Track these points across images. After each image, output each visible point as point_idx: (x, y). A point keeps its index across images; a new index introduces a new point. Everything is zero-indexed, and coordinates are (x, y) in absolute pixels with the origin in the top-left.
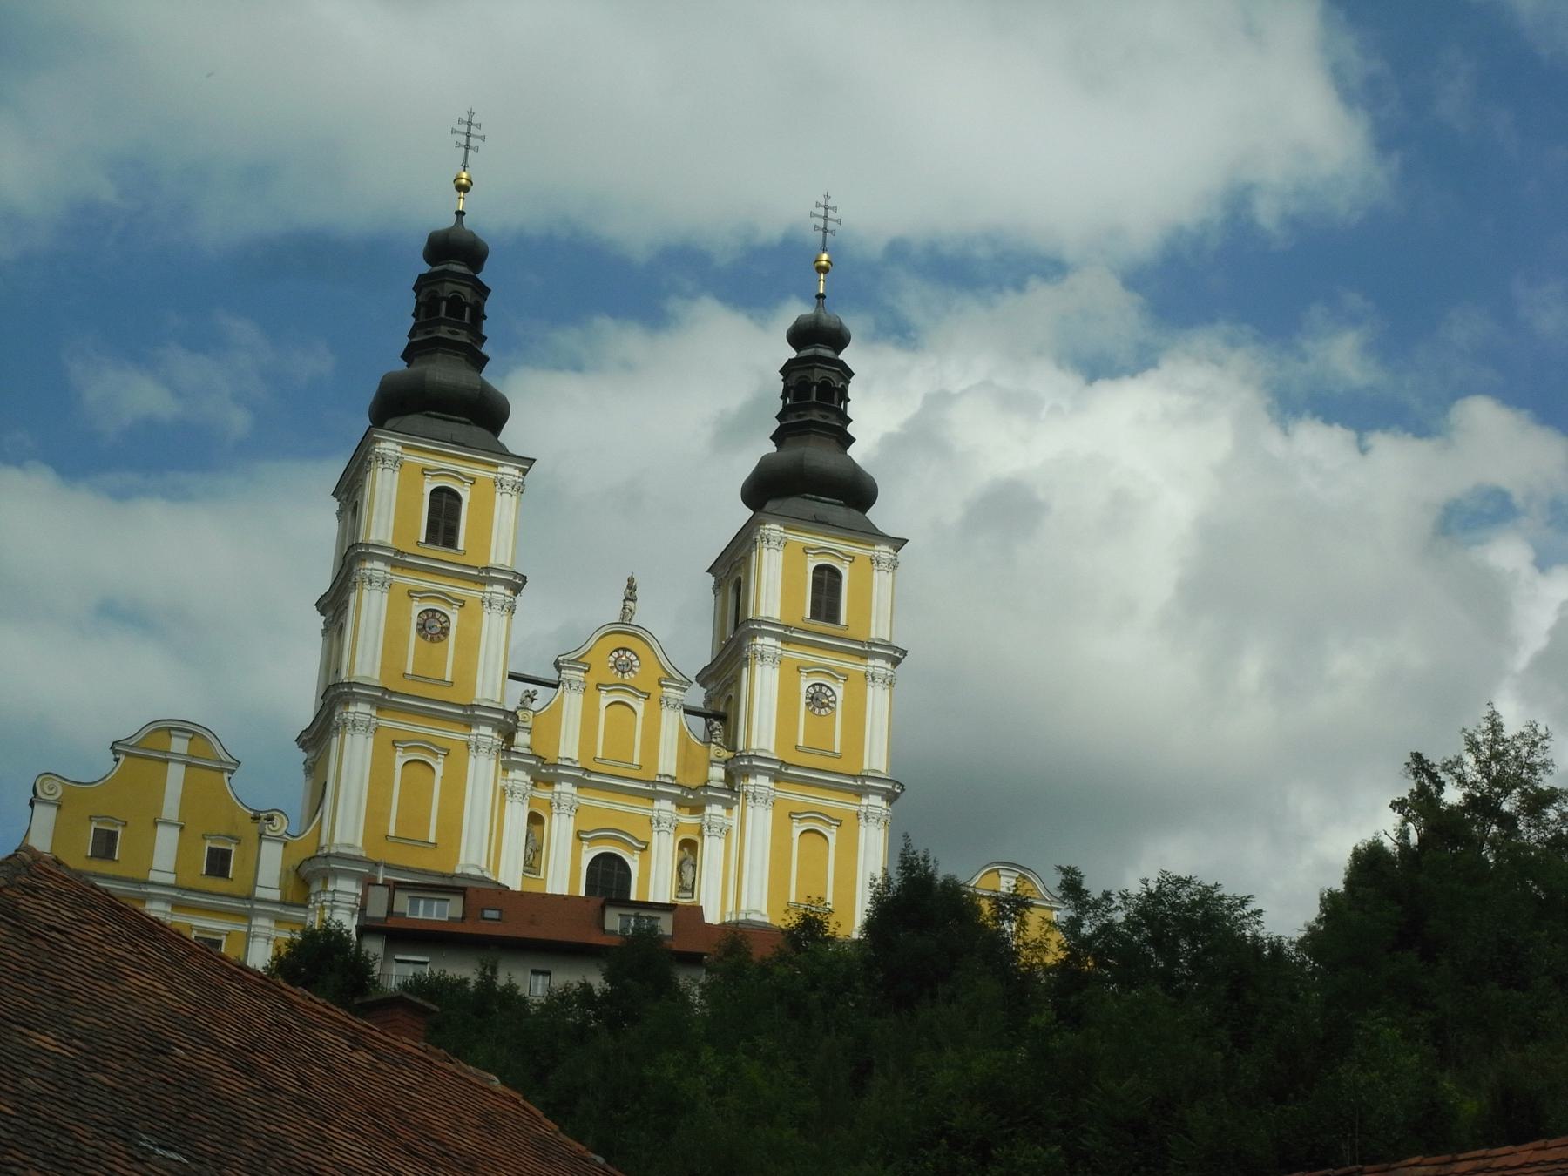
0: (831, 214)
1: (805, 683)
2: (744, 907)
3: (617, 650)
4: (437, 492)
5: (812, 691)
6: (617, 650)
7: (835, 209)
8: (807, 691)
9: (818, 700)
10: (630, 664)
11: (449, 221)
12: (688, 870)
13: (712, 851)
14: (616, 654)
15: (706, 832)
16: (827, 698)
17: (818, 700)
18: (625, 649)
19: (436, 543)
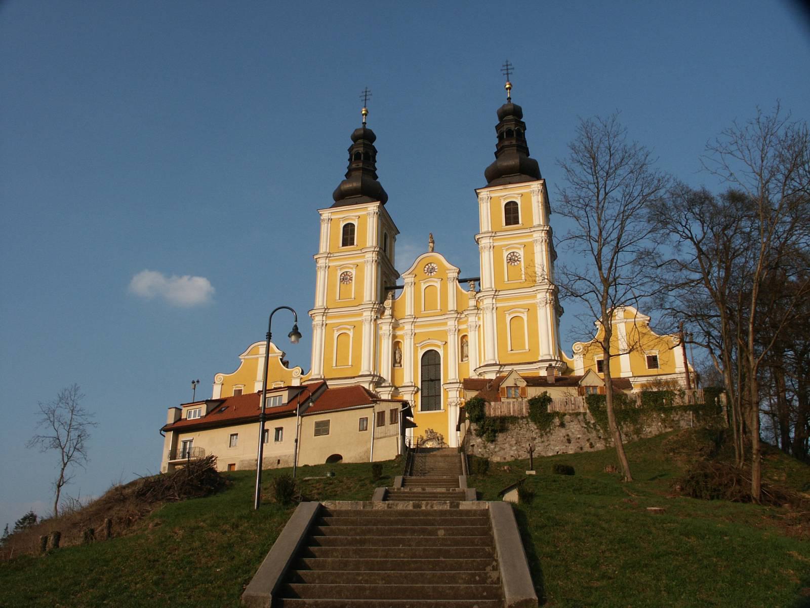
0: (509, 67)
1: (505, 254)
2: (486, 359)
3: (427, 265)
4: (346, 226)
5: (510, 256)
6: (427, 265)
7: (511, 65)
8: (507, 257)
9: (512, 259)
10: (433, 268)
12: (465, 348)
13: (472, 338)
14: (427, 267)
15: (469, 330)
16: (517, 257)
17: (512, 259)
18: (431, 263)
19: (347, 245)
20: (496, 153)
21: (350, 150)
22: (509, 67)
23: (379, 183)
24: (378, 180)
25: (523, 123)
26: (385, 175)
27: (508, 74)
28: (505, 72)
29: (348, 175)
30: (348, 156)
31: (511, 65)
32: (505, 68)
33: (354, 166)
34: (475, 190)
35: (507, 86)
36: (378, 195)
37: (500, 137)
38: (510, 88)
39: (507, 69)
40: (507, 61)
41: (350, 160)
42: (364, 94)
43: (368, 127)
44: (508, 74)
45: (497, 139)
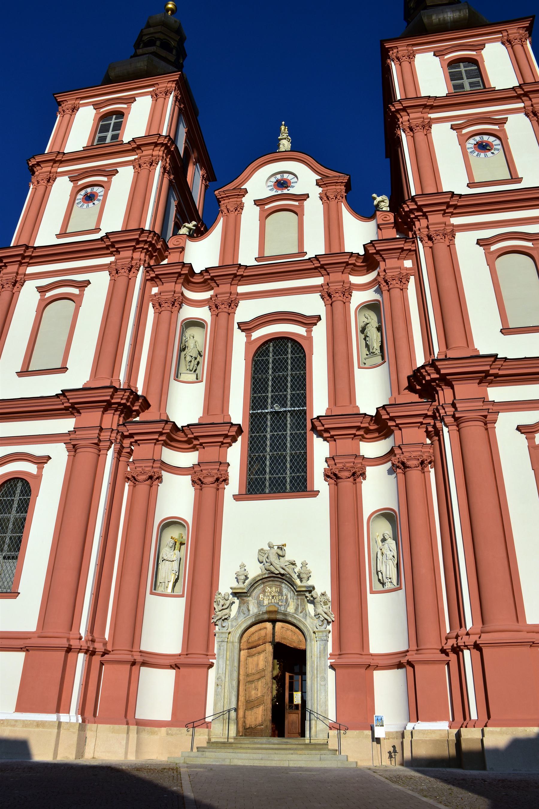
34: (382, 42)
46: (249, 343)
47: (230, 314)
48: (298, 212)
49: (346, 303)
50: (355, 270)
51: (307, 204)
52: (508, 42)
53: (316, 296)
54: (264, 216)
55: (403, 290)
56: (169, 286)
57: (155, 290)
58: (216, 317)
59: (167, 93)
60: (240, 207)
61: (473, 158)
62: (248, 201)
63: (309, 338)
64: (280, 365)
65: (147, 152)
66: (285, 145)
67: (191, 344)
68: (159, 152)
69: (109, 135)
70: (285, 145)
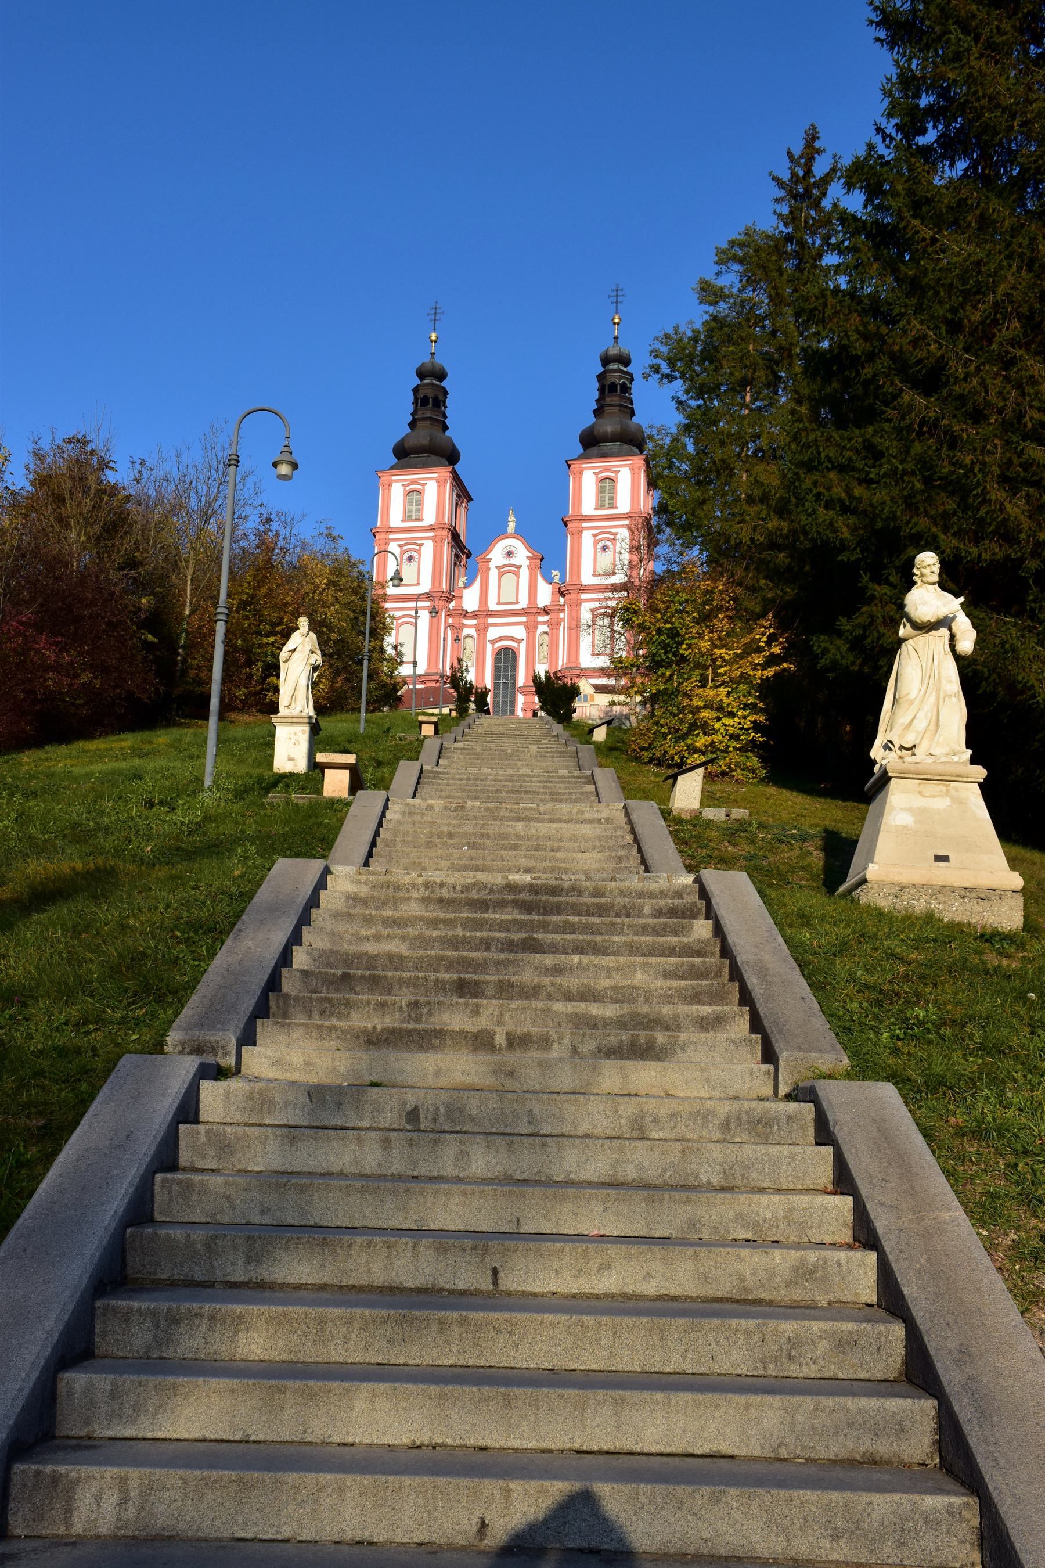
11: (427, 359)
20: (595, 411)
21: (416, 390)
22: (619, 293)
23: (450, 440)
24: (447, 433)
25: (631, 375)
26: (457, 433)
27: (617, 303)
28: (614, 299)
29: (412, 425)
30: (412, 399)
31: (622, 290)
32: (615, 293)
33: (419, 415)
35: (617, 320)
36: (451, 457)
37: (601, 390)
38: (618, 324)
39: (617, 296)
40: (617, 285)
41: (415, 403)
42: (433, 311)
43: (439, 360)
44: (617, 303)
45: (597, 393)
46: (493, 649)
47: (485, 634)
48: (517, 574)
49: (535, 632)
50: (540, 614)
51: (521, 570)
52: (632, 469)
53: (522, 628)
54: (501, 575)
55: (558, 629)
56: (457, 619)
57: (450, 621)
58: (478, 635)
59: (445, 481)
60: (488, 569)
61: (598, 554)
62: (492, 565)
63: (519, 649)
64: (506, 660)
65: (439, 532)
66: (512, 526)
67: (468, 647)
68: (446, 533)
69: (414, 508)
70: (512, 526)
